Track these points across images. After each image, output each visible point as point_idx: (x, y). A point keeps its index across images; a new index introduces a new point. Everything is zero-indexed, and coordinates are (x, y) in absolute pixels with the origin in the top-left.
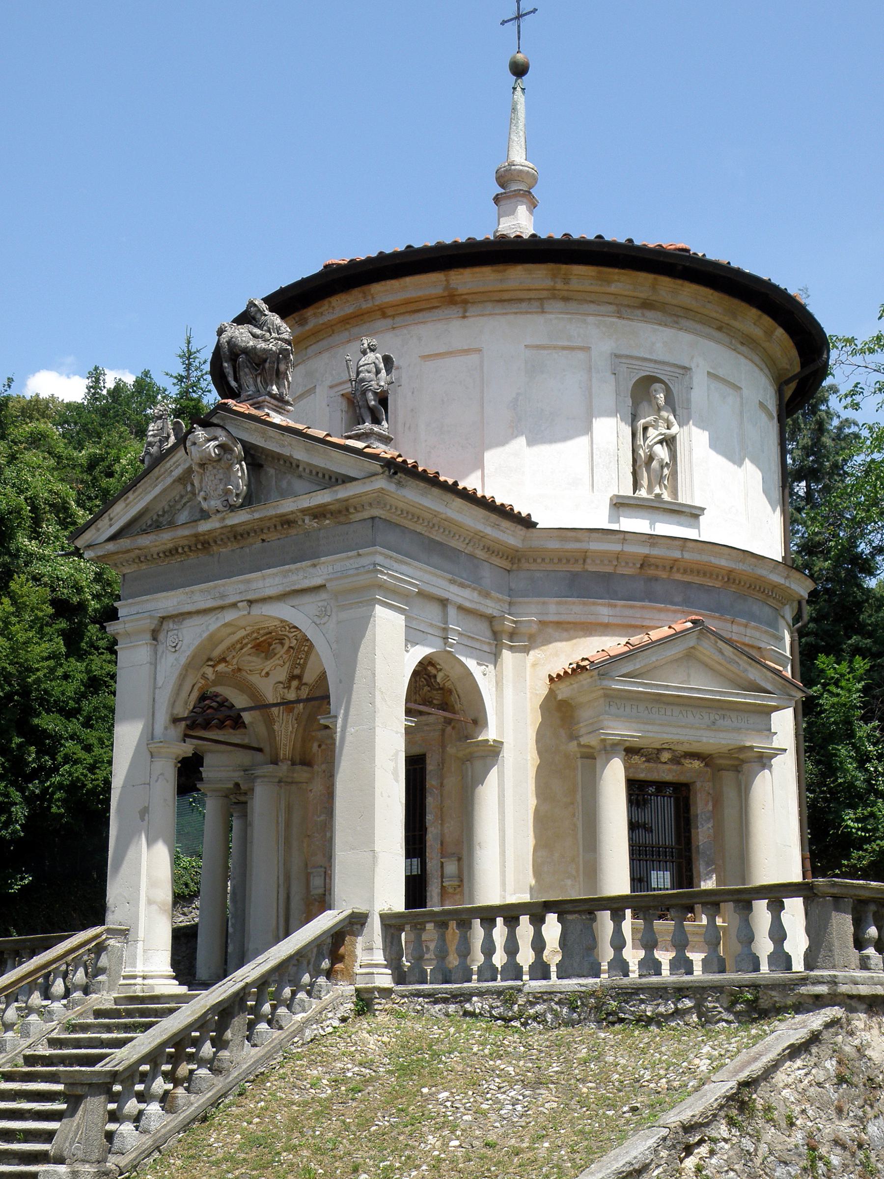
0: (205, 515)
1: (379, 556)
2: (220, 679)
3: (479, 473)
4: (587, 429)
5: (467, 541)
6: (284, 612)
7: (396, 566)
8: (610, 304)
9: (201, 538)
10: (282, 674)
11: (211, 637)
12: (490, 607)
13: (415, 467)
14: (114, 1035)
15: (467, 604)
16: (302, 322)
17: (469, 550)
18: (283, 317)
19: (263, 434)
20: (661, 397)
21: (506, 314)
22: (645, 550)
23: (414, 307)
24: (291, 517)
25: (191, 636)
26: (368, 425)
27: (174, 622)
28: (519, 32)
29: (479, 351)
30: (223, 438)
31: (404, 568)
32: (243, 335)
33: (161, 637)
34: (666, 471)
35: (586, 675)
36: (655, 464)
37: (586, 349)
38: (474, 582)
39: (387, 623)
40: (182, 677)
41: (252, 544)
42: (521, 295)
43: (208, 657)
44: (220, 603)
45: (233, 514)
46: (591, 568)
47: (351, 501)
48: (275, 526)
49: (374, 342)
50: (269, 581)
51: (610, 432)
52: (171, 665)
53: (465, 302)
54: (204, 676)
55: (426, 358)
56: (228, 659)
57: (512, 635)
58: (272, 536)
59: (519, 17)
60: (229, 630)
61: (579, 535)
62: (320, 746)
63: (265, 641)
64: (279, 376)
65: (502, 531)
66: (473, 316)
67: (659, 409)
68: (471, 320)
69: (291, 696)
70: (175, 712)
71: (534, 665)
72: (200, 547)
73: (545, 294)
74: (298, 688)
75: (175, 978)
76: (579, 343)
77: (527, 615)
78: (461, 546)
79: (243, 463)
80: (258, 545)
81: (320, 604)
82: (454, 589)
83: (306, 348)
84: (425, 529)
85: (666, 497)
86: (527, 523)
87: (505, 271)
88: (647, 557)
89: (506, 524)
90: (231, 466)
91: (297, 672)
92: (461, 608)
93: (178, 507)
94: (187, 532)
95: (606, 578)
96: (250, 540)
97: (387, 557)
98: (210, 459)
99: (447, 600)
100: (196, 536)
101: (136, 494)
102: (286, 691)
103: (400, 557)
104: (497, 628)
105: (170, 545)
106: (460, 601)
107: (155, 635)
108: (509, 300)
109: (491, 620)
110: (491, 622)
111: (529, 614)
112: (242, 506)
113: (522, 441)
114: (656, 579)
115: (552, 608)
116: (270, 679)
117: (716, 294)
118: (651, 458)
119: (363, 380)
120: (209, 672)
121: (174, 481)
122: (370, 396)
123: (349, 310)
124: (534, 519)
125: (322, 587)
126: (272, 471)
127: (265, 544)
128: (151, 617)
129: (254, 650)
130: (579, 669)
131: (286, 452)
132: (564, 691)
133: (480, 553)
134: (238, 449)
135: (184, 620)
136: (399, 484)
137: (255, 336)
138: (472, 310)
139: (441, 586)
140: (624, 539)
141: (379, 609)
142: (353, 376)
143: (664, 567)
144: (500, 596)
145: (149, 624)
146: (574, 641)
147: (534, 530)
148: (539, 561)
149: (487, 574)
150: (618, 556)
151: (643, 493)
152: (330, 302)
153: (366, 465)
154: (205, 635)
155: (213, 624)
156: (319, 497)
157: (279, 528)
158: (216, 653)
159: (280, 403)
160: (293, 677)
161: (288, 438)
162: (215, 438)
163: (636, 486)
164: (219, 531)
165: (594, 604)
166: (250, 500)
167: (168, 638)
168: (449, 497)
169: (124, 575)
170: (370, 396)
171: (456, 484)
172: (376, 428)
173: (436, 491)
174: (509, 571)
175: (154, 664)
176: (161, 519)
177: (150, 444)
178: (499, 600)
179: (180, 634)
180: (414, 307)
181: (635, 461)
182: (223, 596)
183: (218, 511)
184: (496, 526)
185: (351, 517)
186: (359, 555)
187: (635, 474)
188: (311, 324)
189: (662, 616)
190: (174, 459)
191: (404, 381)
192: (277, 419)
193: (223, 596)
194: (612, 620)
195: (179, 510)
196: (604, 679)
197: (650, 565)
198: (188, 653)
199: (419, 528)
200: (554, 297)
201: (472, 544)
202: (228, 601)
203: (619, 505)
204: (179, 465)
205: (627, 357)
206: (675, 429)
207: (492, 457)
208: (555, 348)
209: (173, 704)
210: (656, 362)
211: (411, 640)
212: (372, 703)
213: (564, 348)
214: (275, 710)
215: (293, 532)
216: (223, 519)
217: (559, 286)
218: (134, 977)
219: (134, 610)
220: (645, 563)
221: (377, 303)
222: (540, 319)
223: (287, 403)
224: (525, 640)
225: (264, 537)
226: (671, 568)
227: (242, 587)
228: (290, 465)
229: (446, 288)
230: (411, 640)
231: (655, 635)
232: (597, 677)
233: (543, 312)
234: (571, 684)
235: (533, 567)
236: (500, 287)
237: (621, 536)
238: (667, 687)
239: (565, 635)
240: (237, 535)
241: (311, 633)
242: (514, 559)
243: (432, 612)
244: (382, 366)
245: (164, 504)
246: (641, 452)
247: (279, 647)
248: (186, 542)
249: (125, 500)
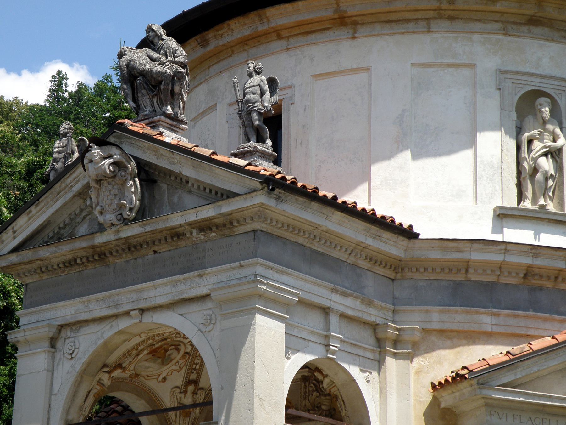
0: (102, 228)
1: (260, 267)
2: (116, 384)
3: (366, 185)
4: (472, 143)
5: (349, 252)
6: (172, 321)
7: (276, 276)
8: (496, 21)
9: (98, 249)
10: (178, 379)
11: (105, 344)
12: (373, 315)
13: (294, 183)
15: (350, 312)
16: (204, 43)
17: (351, 260)
18: (181, 42)
19: (156, 152)
20: (546, 110)
21: (394, 34)
22: (527, 260)
23: (307, 28)
24: (180, 230)
25: (87, 343)
26: (252, 143)
29: (367, 69)
30: (117, 156)
31: (285, 278)
32: (142, 59)
33: (59, 344)
34: (550, 183)
35: (465, 384)
36: (539, 176)
37: (472, 66)
38: (358, 291)
39: (267, 332)
40: (78, 383)
41: (144, 256)
42: (408, 15)
43: (102, 364)
45: (126, 227)
46: (474, 277)
47: (234, 215)
48: (166, 239)
49: (260, 65)
50: (159, 291)
51: (495, 146)
52: (67, 371)
53: (355, 24)
54: (100, 383)
55: (318, 77)
56: (124, 365)
57: (396, 343)
58: (163, 248)
60: (123, 337)
61: (461, 245)
63: (161, 347)
64: (174, 97)
65: (384, 242)
66: (363, 37)
67: (545, 122)
68: (360, 40)
69: (188, 400)
70: (70, 418)
71: (418, 372)
72: (96, 258)
73: (431, 14)
74: (194, 393)
77: (411, 322)
78: (342, 256)
79: (137, 179)
80: (151, 256)
81: (206, 312)
82: (336, 297)
83: (209, 68)
84: (307, 240)
85: (551, 207)
86: (409, 234)
88: (530, 267)
89: (387, 235)
90: (126, 181)
91: (193, 376)
92: (343, 316)
93: (79, 220)
94: (84, 244)
95: (489, 288)
96: (143, 251)
97: (267, 267)
98: (105, 176)
99: (329, 308)
100: (93, 247)
101: (38, 208)
102: (183, 395)
103: (280, 268)
104: (381, 335)
105: (69, 257)
106: (342, 309)
107: (53, 342)
108: (397, 21)
109: (374, 327)
110: (375, 330)
111: (412, 322)
112: (135, 219)
113: (407, 154)
114: (541, 288)
115: (435, 316)
116: (166, 384)
118: (535, 170)
119: (248, 101)
120: (105, 378)
121: (74, 196)
122: (255, 116)
123: (246, 32)
124: (415, 230)
125: (207, 296)
126: (164, 187)
127: (157, 255)
128: (50, 325)
129: (150, 356)
130: (458, 378)
131: (176, 169)
132: (448, 399)
133: (363, 263)
134: (132, 166)
135: (80, 327)
136: (279, 198)
137: (152, 59)
138: (361, 31)
139: (321, 294)
140: (506, 250)
141: (259, 319)
142: (240, 97)
143: (549, 277)
144: (383, 304)
145: (47, 332)
146: (458, 349)
147: (415, 241)
148: (422, 270)
149: (370, 284)
150: (501, 266)
151: (527, 204)
152: (229, 25)
153: (247, 181)
154: (100, 342)
155: (107, 331)
156: (205, 212)
157: (169, 240)
158: (112, 359)
159: (175, 122)
160: (189, 382)
161: (178, 156)
162: (110, 157)
163: (521, 197)
164: (114, 243)
165: (477, 313)
166: (142, 214)
167: (65, 346)
168: (328, 210)
170: (255, 116)
171: (335, 198)
172: (260, 147)
173: (315, 205)
174: (393, 280)
175: (51, 371)
176: (62, 231)
177: (55, 160)
178: (382, 308)
179: (76, 341)
180: (307, 28)
181: (519, 173)
182: (117, 305)
183: (113, 225)
184: (376, 237)
185: (235, 229)
186: (241, 266)
187: (520, 186)
188: (211, 46)
189: (548, 325)
190: (74, 175)
191: (297, 99)
192: (169, 137)
193: (117, 305)
194: (496, 329)
195: (79, 223)
196: (484, 388)
197: (534, 275)
199: (300, 240)
200: (440, 17)
201: (354, 254)
203: (503, 216)
204: (79, 181)
205: (513, 72)
206: (561, 142)
207: (378, 171)
208: (441, 65)
209: (68, 411)
210: (542, 76)
211: (290, 348)
212: (251, 410)
213: (450, 65)
214: (172, 414)
215: (182, 243)
216: (118, 231)
217: (445, 6)
219: (34, 318)
220: (529, 273)
221: (272, 25)
222: (426, 38)
223: (182, 122)
224: (409, 347)
225: (156, 248)
226: (556, 278)
227: (135, 296)
228: (181, 181)
229: (336, 11)
230: (290, 348)
231: (537, 345)
232: (476, 386)
233: (429, 31)
234: (453, 392)
235: (417, 276)
236: (387, 8)
237: (503, 247)
238: (550, 398)
239: (448, 342)
240: (131, 247)
242: (398, 268)
243: (314, 320)
244: (266, 87)
245: (65, 217)
246: (526, 164)
247: (175, 352)
248: (84, 254)
249: (28, 214)
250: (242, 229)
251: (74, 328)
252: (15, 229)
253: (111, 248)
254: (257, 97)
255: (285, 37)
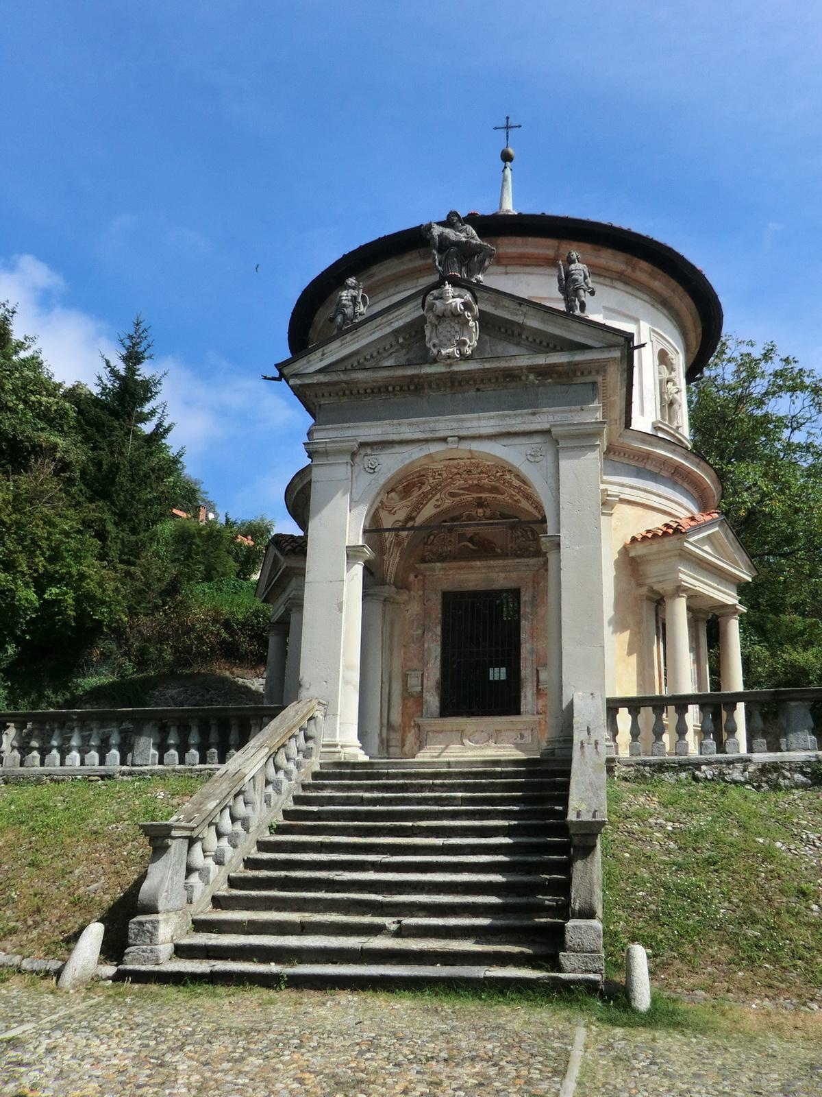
6: (496, 450)
14: (437, 794)
25: (391, 464)
27: (372, 449)
28: (507, 136)
33: (357, 459)
44: (429, 435)
48: (497, 378)
50: (485, 422)
59: (507, 127)
62: (416, 577)
72: (412, 387)
75: (361, 748)
76: (633, 314)
81: (533, 446)
83: (417, 279)
87: (599, 251)
117: (696, 310)
127: (478, 393)
154: (407, 462)
155: (415, 454)
157: (501, 380)
169: (320, 406)
176: (366, 363)
185: (574, 379)
195: (384, 358)
198: (389, 475)
202: (438, 435)
216: (451, 365)
218: (335, 746)
222: (612, 291)
225: (481, 386)
235: (616, 458)
241: (525, 469)
247: (417, 489)
249: (342, 340)
250: (581, 380)
251: (375, 447)
252: (325, 351)
253: (431, 382)
254: (581, 278)
255: (503, 265)
